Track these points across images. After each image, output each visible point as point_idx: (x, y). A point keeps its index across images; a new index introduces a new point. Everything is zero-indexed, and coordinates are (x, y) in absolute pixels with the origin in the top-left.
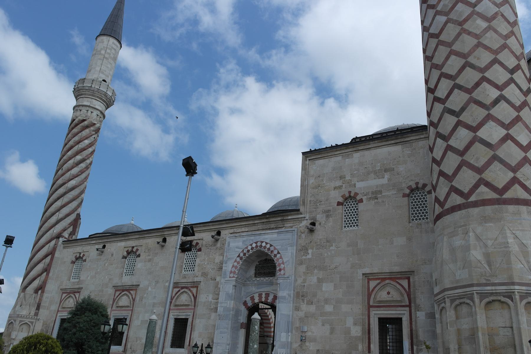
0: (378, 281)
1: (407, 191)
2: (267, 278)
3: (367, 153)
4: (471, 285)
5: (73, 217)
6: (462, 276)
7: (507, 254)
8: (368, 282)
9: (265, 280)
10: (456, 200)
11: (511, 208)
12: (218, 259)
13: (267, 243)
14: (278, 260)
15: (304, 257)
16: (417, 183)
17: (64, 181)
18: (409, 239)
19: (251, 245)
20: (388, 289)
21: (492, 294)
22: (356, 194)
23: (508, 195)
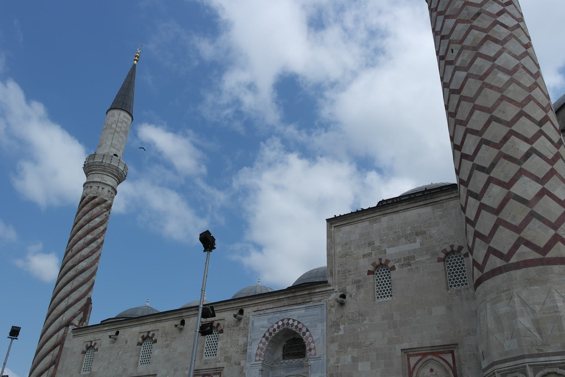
0: (419, 357)
1: (442, 255)
2: (296, 360)
3: (395, 216)
4: (523, 357)
5: (83, 302)
8: (408, 359)
9: (294, 362)
10: (495, 262)
11: (557, 268)
12: (242, 341)
13: (294, 320)
14: (307, 338)
15: (335, 334)
16: (452, 246)
17: (74, 263)
18: (449, 308)
19: (277, 323)
20: (431, 365)
21: (546, 365)
22: (387, 261)
23: (551, 254)
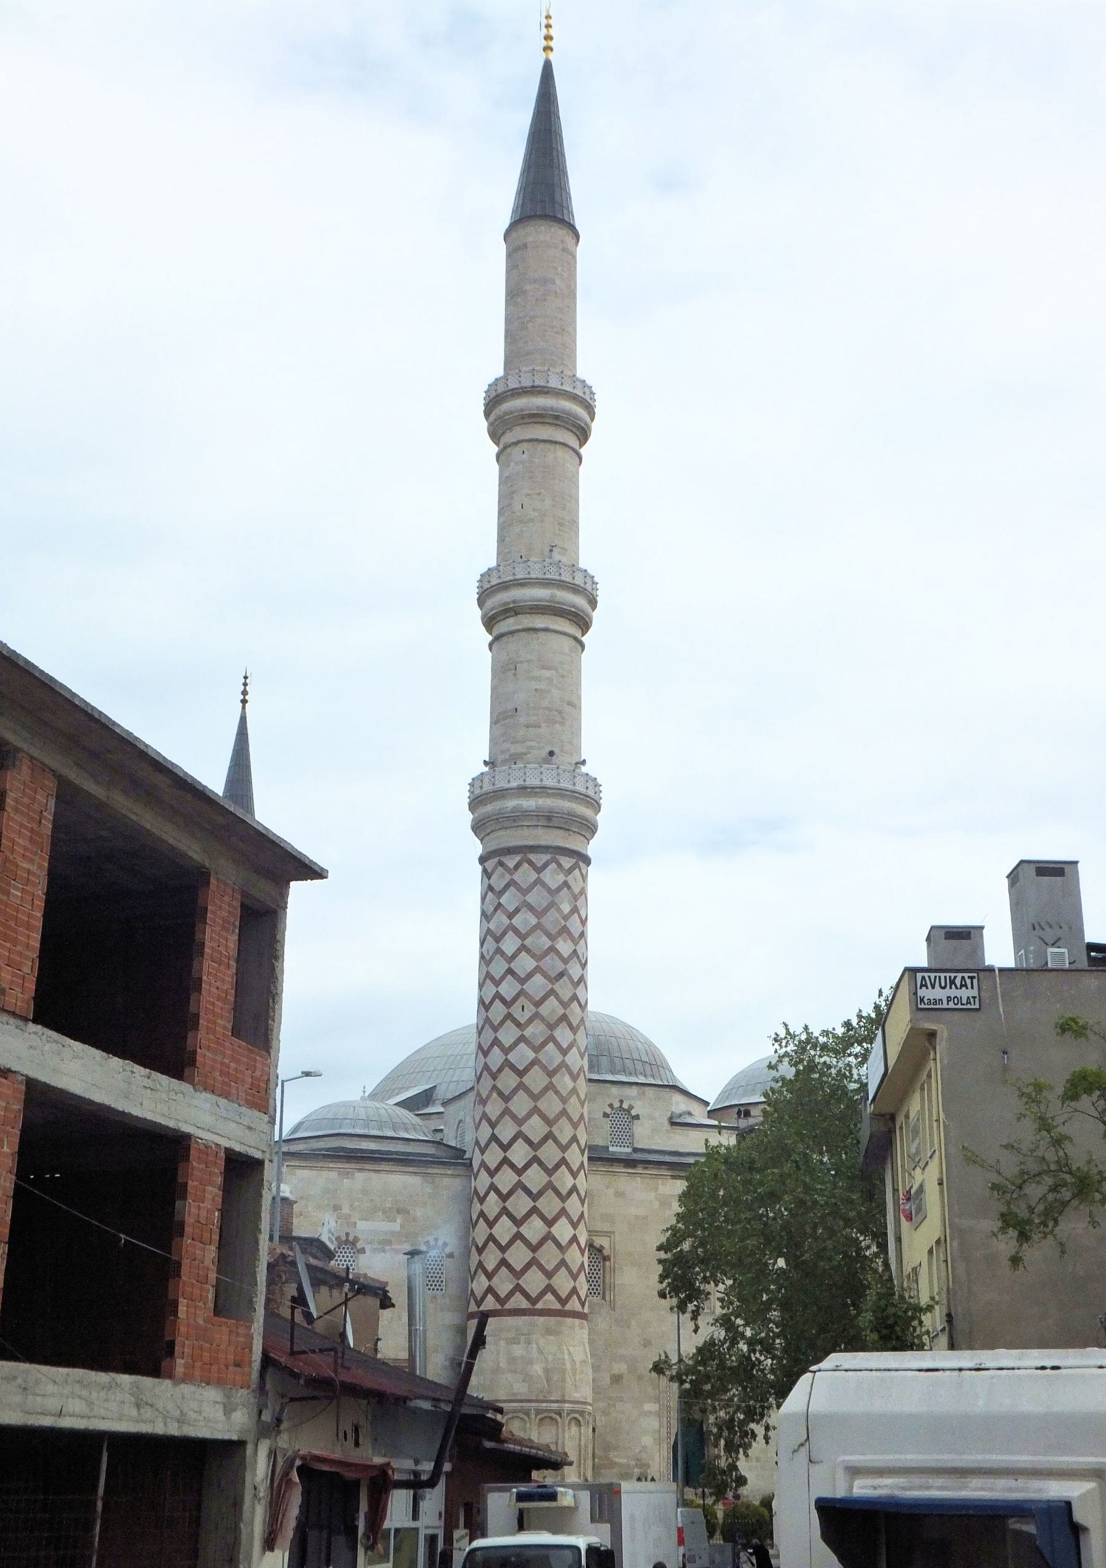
3: (373, 1175)
4: (530, 1401)
6: (521, 1389)
7: (563, 1371)
11: (569, 1321)
23: (568, 1307)
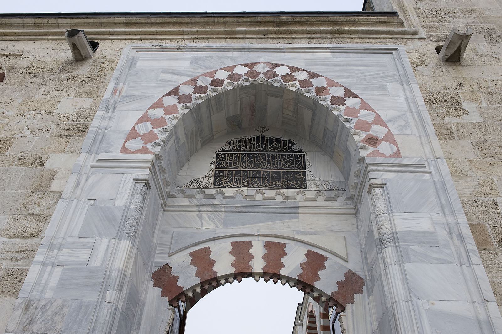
2: (270, 192)
